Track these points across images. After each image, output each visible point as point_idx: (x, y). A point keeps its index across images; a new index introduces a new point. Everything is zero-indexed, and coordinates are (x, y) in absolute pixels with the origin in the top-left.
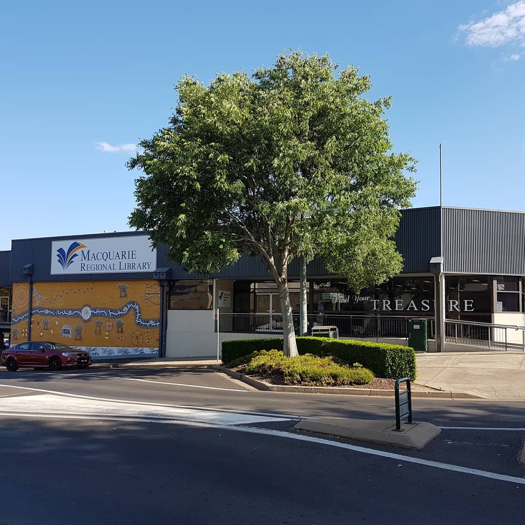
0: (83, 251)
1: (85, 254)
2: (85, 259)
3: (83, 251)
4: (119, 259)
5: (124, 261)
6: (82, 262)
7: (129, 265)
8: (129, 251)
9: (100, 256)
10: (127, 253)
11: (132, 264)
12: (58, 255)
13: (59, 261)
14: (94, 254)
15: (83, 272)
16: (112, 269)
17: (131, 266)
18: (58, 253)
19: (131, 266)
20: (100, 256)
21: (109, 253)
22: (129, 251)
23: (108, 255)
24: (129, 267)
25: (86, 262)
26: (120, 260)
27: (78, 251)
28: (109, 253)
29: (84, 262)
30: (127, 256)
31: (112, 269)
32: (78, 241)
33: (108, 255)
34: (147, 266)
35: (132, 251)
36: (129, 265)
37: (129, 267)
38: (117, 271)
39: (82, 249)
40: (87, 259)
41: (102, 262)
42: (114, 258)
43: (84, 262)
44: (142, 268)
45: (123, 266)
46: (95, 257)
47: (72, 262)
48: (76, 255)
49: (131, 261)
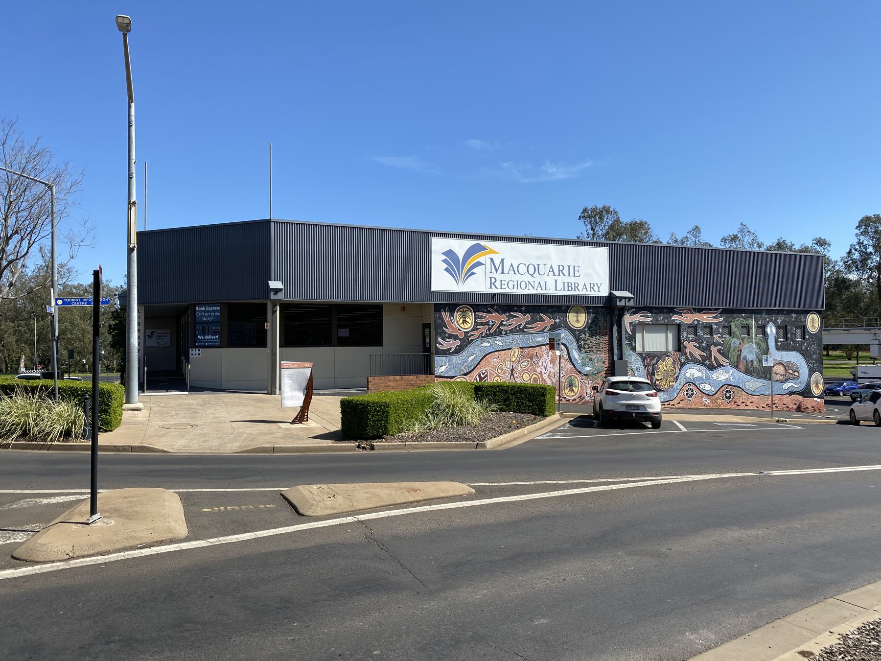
0: (492, 260)
1: (497, 262)
2: (497, 271)
3: (492, 260)
4: (554, 275)
5: (561, 280)
6: (491, 275)
7: (570, 285)
8: (569, 266)
9: (522, 269)
10: (566, 269)
11: (573, 284)
12: (444, 261)
13: (447, 270)
14: (512, 265)
15: (494, 291)
16: (544, 288)
17: (573, 286)
18: (444, 257)
19: (573, 286)
20: (522, 269)
21: (538, 265)
22: (569, 266)
23: (537, 269)
24: (570, 289)
25: (498, 276)
26: (556, 277)
27: (484, 259)
28: (538, 265)
29: (494, 275)
30: (566, 272)
31: (544, 288)
32: (483, 243)
33: (537, 269)
34: (596, 288)
35: (574, 267)
36: (570, 285)
37: (570, 289)
38: (552, 292)
39: (491, 256)
40: (500, 270)
41: (527, 278)
42: (547, 273)
43: (494, 275)
44: (589, 289)
45: (560, 286)
46: (514, 270)
47: (473, 273)
48: (479, 264)
49: (572, 280)
